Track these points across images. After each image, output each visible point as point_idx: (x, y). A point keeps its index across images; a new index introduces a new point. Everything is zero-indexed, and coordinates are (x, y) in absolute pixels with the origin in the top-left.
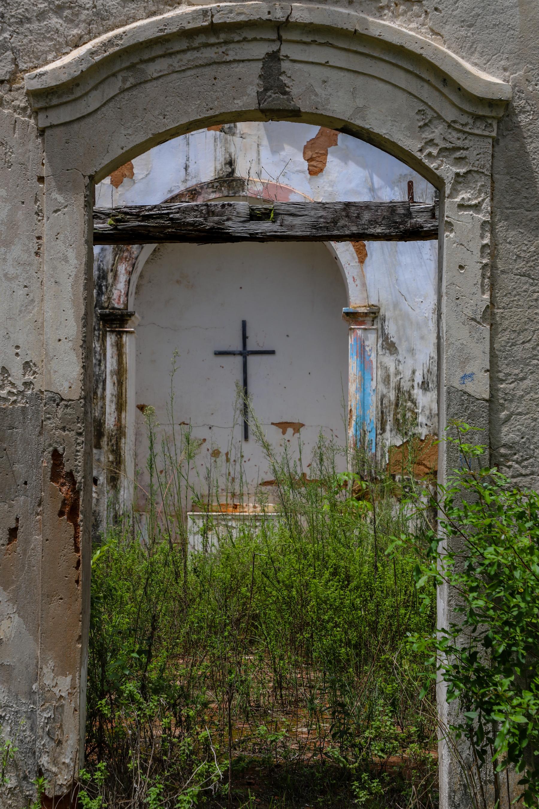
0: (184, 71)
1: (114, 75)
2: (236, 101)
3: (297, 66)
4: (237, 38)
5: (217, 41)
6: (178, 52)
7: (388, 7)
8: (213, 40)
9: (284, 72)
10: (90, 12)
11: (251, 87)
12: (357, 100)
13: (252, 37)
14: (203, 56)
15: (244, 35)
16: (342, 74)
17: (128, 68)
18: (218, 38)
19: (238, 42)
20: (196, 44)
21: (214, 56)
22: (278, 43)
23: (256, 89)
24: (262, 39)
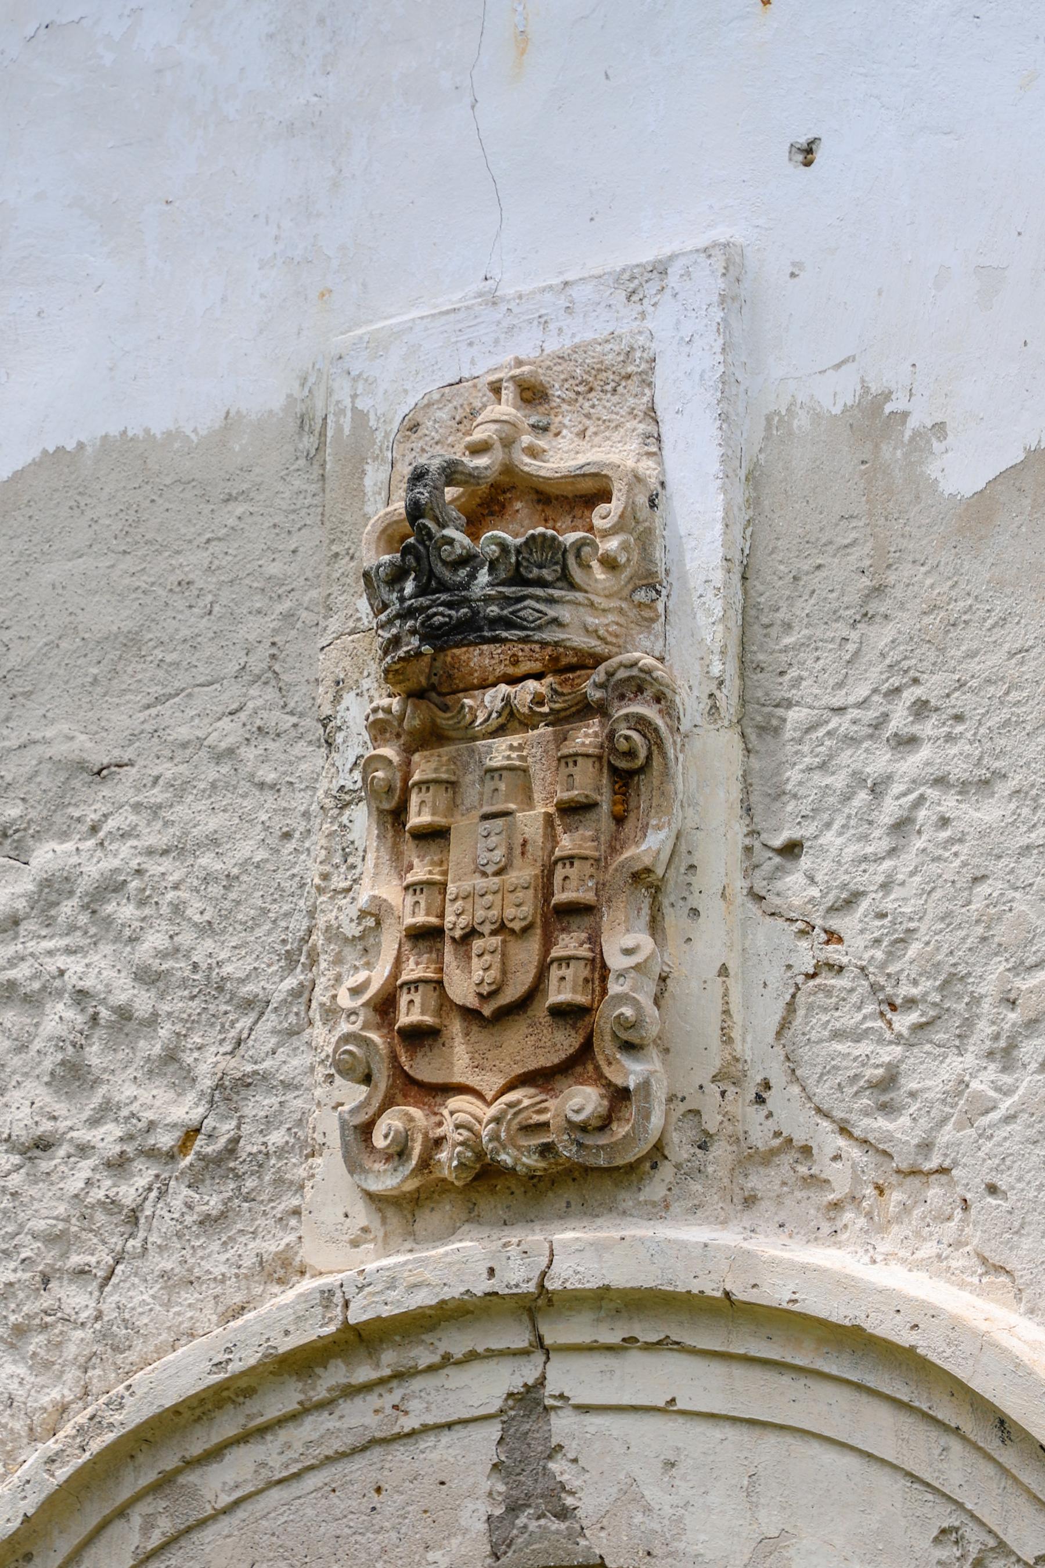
0: (297, 1476)
1: (121, 1513)
2: (431, 1556)
3: (595, 1422)
4: (425, 1358)
5: (374, 1375)
6: (281, 1422)
7: (854, 1199)
8: (365, 1373)
9: (560, 1447)
10: (87, 1334)
11: (471, 1506)
12: (762, 1514)
13: (465, 1350)
14: (345, 1424)
15: (443, 1347)
16: (716, 1432)
17: (155, 1488)
18: (378, 1366)
19: (431, 1369)
20: (320, 1392)
21: (371, 1421)
22: (539, 1358)
23: (484, 1508)
24: (491, 1354)
